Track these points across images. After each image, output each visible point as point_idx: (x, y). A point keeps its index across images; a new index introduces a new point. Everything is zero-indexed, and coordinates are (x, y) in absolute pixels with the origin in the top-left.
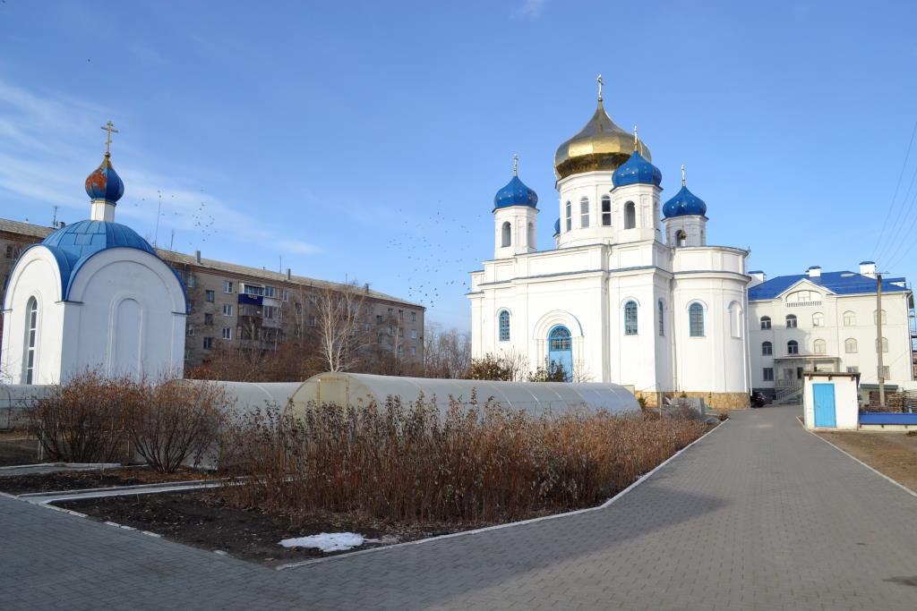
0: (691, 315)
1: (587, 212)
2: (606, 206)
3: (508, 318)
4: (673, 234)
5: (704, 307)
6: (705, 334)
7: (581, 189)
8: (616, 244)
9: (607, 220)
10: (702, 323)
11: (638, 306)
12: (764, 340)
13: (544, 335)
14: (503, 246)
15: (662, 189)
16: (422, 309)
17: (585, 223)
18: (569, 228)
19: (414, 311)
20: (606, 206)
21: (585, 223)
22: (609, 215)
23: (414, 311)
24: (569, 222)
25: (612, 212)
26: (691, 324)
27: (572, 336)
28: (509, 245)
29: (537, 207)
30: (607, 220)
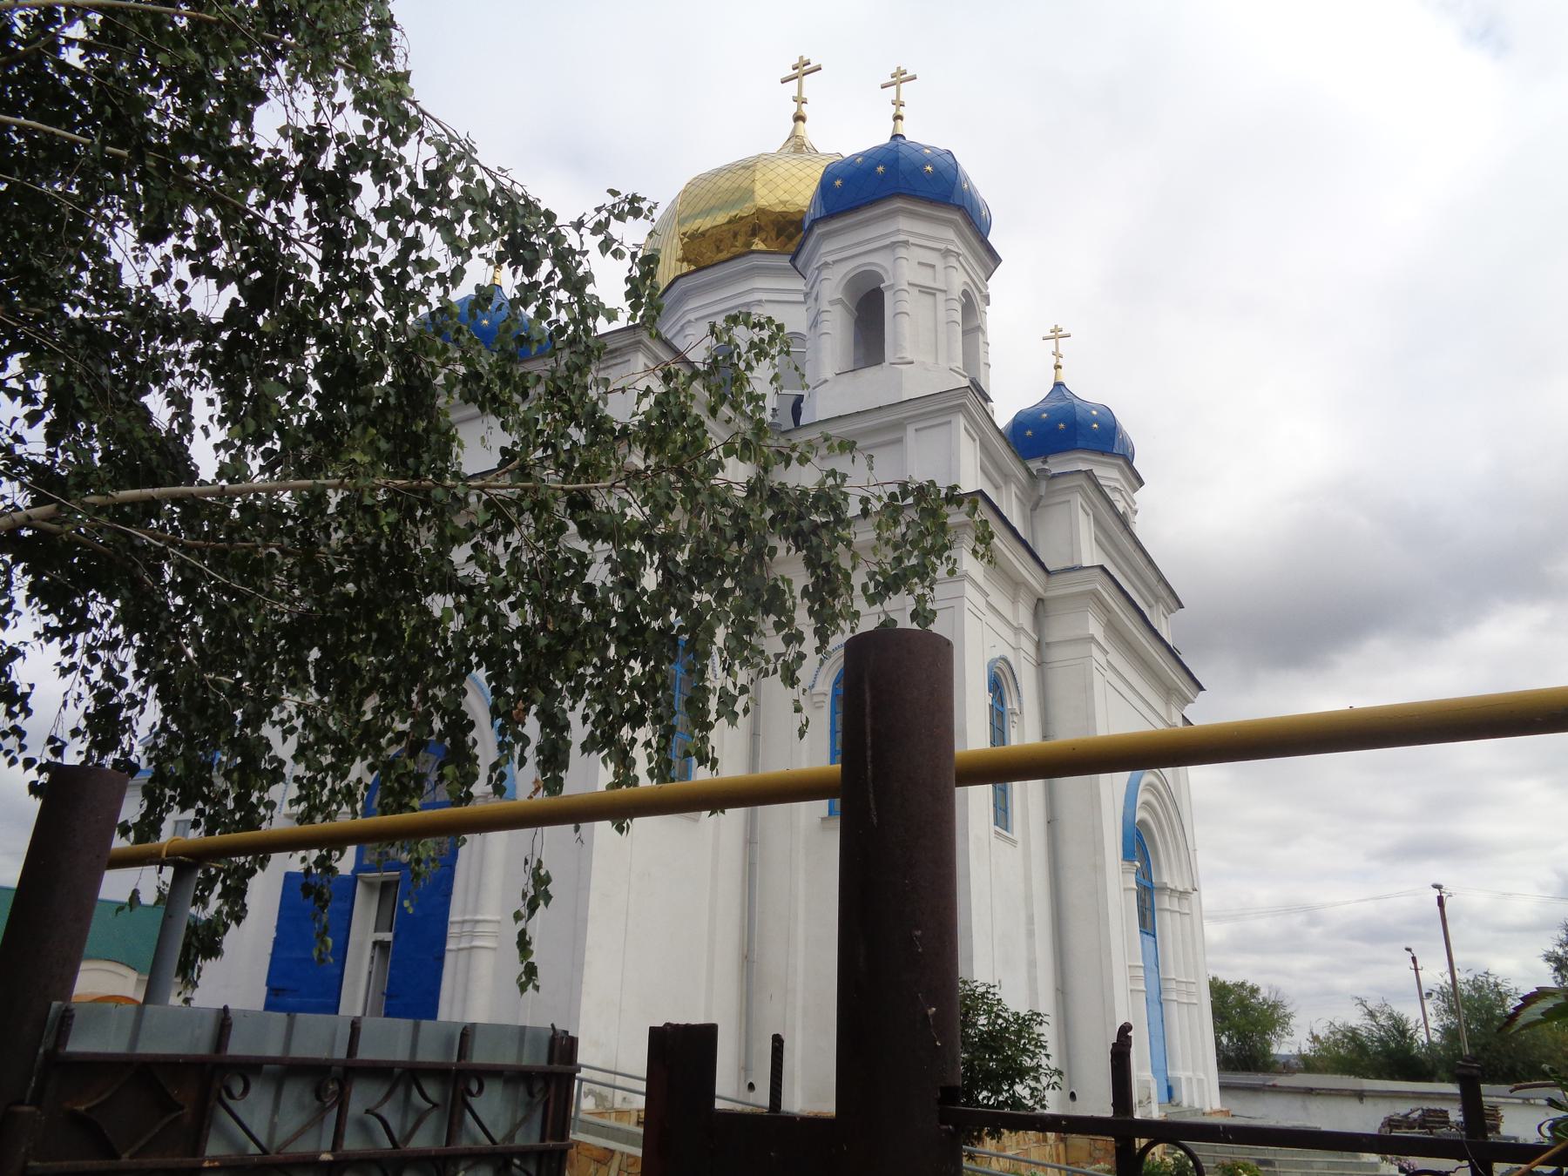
15: (996, 259)
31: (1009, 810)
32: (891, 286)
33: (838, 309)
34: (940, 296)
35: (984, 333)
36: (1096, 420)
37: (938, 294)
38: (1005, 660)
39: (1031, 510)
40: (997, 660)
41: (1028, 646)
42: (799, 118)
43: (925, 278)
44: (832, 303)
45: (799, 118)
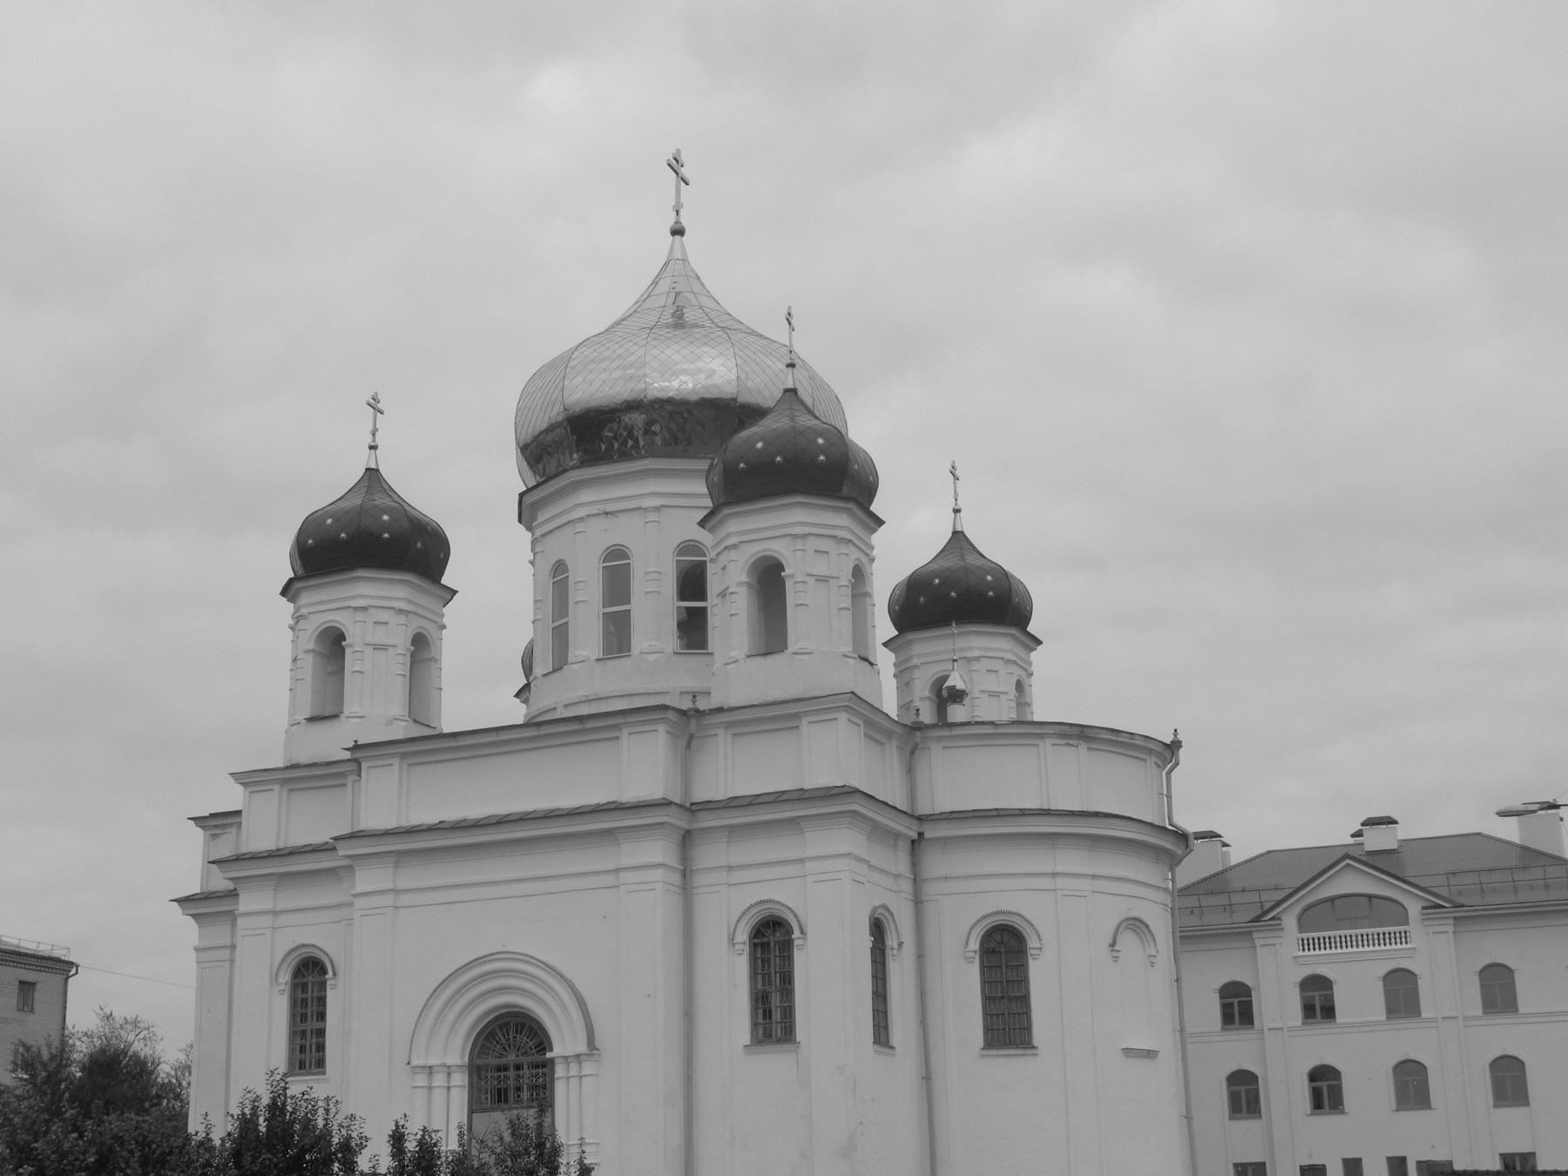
0: (985, 968)
1: (629, 603)
2: (692, 582)
3: (322, 986)
4: (922, 688)
5: (1032, 943)
6: (1036, 1041)
7: (601, 522)
8: (720, 710)
9: (693, 629)
10: (1025, 999)
11: (796, 934)
12: (1233, 1068)
13: (456, 1052)
14: (311, 720)
15: (880, 522)
16: (62, 968)
17: (617, 636)
18: (560, 663)
19: (29, 976)
20: (692, 582)
21: (617, 636)
22: (703, 611)
23: (29, 976)
24: (561, 636)
25: (712, 602)
26: (987, 999)
27: (558, 1050)
28: (335, 716)
29: (443, 581)
30: (693, 629)
31: (890, 1028)
32: (792, 576)
33: (743, 590)
34: (831, 581)
35: (870, 595)
36: (990, 586)
37: (831, 581)
38: (884, 907)
39: (910, 754)
40: (878, 907)
41: (906, 886)
42: (678, 231)
43: (821, 568)
44: (739, 584)
45: (678, 231)
